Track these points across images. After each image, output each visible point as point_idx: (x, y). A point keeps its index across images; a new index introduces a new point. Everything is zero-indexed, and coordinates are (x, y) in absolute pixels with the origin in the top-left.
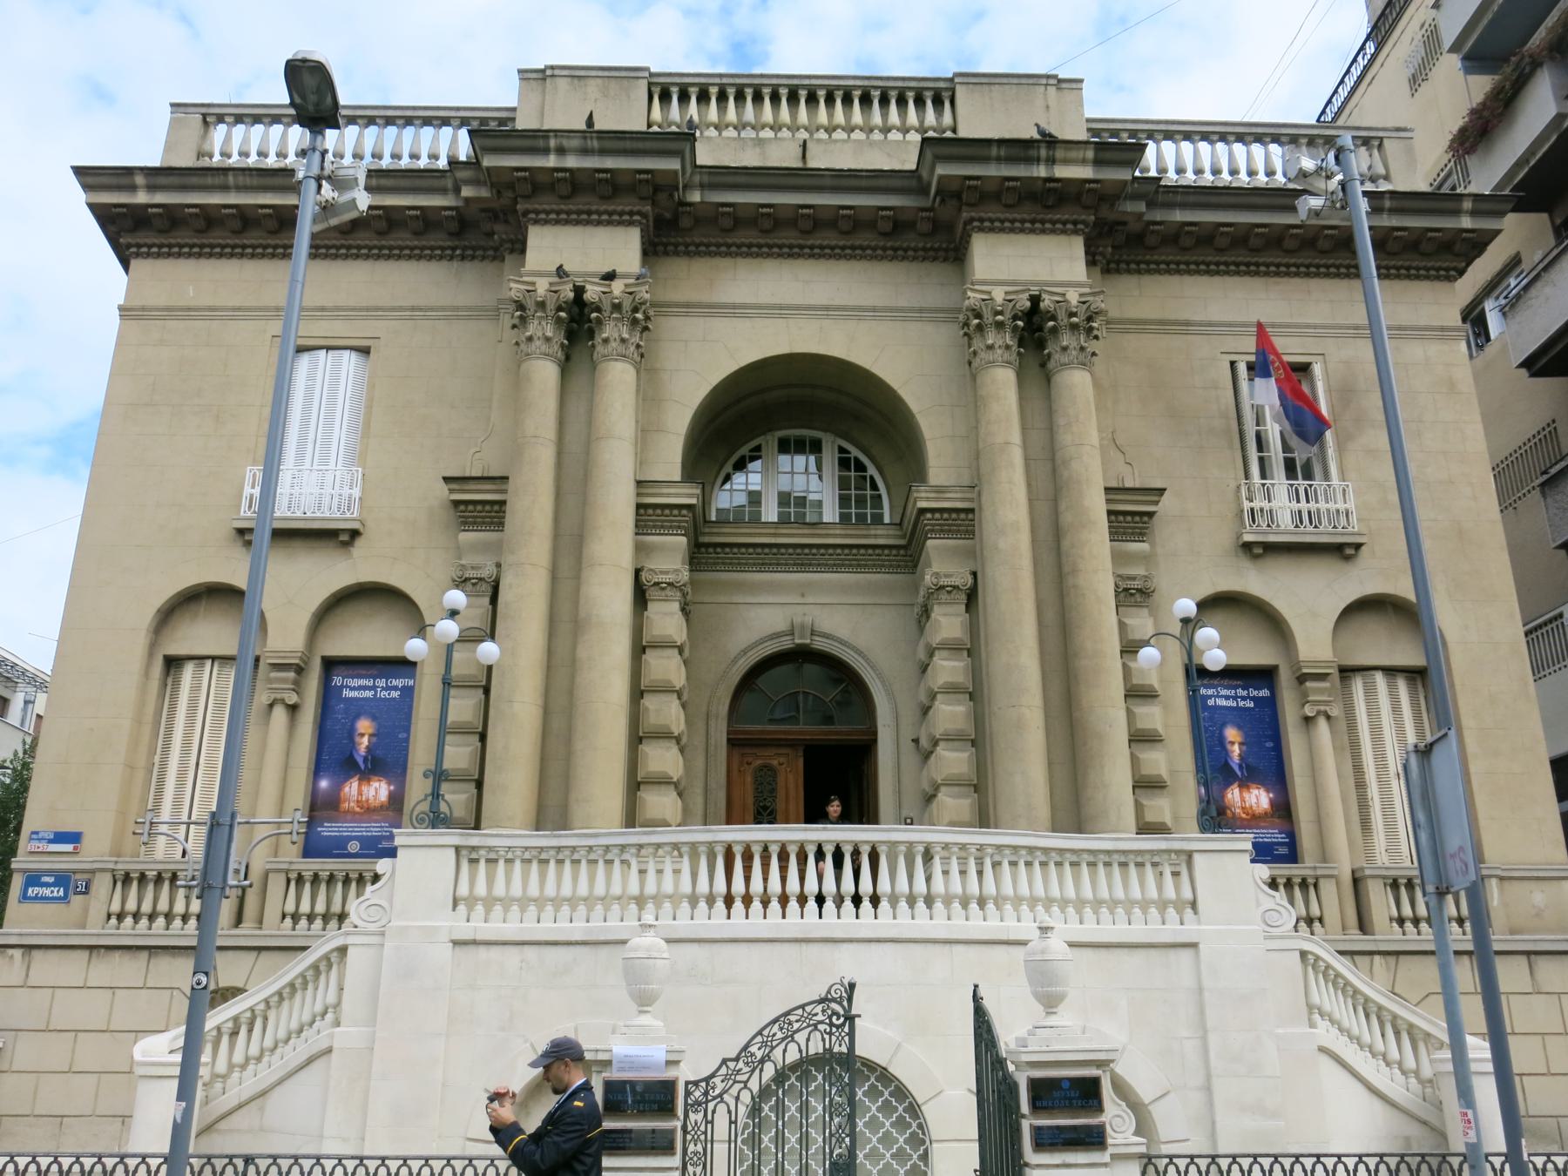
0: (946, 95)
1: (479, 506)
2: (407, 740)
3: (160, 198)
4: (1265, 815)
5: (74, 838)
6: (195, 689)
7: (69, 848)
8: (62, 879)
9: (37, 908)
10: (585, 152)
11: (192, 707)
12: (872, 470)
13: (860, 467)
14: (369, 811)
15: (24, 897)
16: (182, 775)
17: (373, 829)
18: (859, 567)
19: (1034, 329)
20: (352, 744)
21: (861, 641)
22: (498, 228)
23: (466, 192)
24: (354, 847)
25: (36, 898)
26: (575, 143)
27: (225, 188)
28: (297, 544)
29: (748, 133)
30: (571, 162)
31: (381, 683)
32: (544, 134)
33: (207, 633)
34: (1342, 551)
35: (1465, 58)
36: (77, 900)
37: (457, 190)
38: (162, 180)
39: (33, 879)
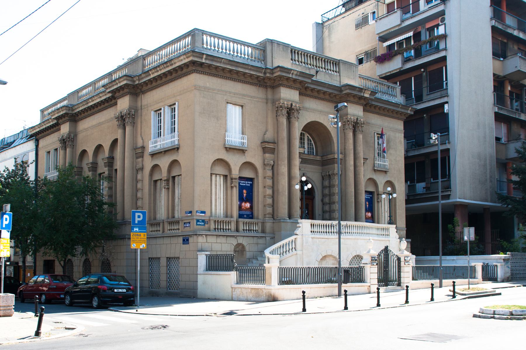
0: (337, 63)
1: (268, 147)
2: (252, 195)
3: (207, 62)
4: (369, 218)
5: (204, 212)
6: (216, 181)
7: (203, 215)
8: (203, 221)
9: (199, 227)
10: (296, 75)
11: (216, 185)
12: (312, 142)
13: (311, 141)
14: (247, 209)
15: (197, 224)
16: (216, 200)
17: (248, 213)
18: (313, 164)
19: (356, 126)
20: (243, 195)
21: (313, 179)
22: (269, 82)
23: (268, 75)
24: (245, 216)
25: (199, 225)
26: (295, 73)
27: (221, 62)
28: (235, 151)
29: (307, 66)
30: (294, 77)
31: (246, 182)
32: (291, 70)
33: (220, 170)
34: (386, 172)
35: (379, 37)
36: (206, 225)
37: (265, 73)
38: (209, 58)
39: (198, 221)
